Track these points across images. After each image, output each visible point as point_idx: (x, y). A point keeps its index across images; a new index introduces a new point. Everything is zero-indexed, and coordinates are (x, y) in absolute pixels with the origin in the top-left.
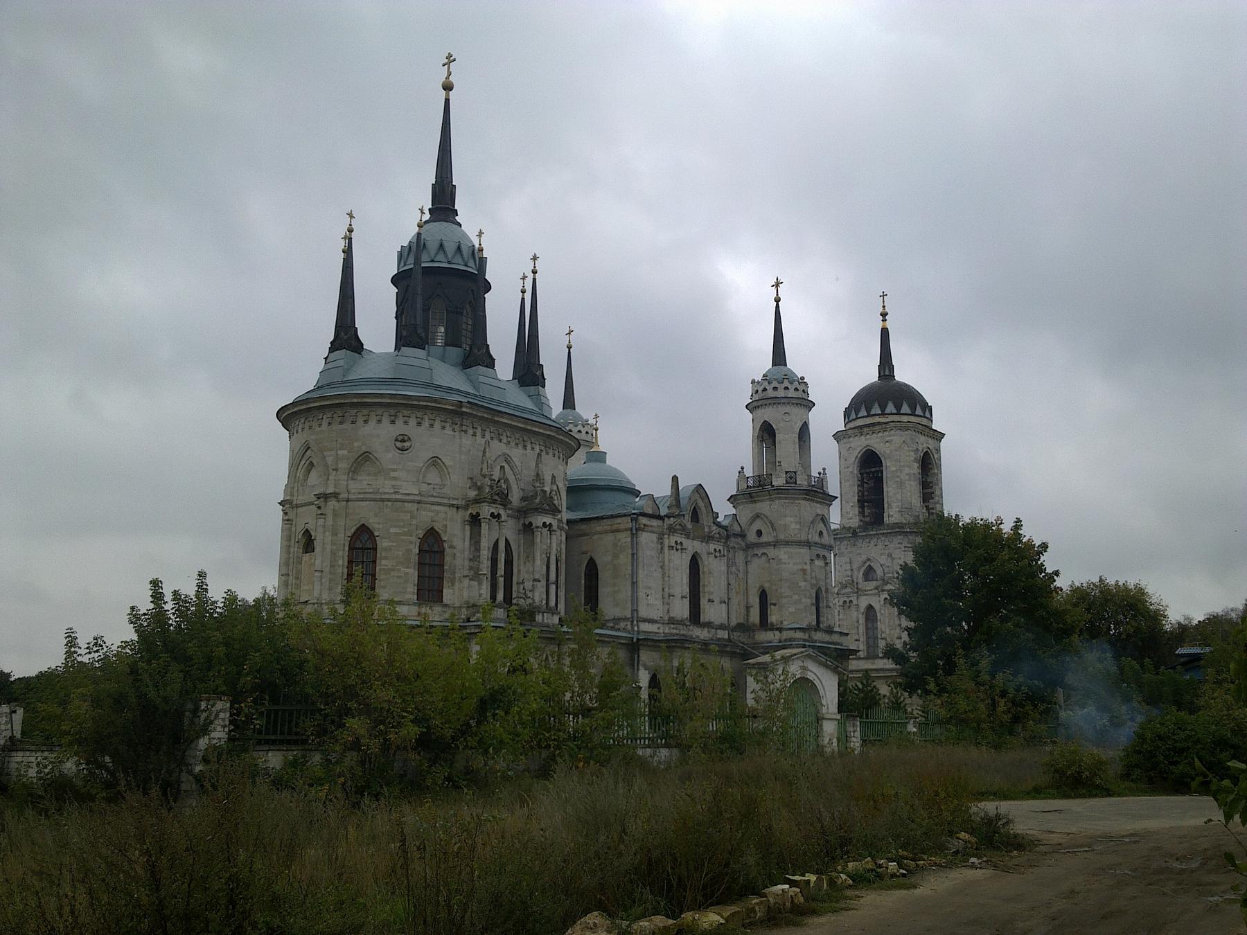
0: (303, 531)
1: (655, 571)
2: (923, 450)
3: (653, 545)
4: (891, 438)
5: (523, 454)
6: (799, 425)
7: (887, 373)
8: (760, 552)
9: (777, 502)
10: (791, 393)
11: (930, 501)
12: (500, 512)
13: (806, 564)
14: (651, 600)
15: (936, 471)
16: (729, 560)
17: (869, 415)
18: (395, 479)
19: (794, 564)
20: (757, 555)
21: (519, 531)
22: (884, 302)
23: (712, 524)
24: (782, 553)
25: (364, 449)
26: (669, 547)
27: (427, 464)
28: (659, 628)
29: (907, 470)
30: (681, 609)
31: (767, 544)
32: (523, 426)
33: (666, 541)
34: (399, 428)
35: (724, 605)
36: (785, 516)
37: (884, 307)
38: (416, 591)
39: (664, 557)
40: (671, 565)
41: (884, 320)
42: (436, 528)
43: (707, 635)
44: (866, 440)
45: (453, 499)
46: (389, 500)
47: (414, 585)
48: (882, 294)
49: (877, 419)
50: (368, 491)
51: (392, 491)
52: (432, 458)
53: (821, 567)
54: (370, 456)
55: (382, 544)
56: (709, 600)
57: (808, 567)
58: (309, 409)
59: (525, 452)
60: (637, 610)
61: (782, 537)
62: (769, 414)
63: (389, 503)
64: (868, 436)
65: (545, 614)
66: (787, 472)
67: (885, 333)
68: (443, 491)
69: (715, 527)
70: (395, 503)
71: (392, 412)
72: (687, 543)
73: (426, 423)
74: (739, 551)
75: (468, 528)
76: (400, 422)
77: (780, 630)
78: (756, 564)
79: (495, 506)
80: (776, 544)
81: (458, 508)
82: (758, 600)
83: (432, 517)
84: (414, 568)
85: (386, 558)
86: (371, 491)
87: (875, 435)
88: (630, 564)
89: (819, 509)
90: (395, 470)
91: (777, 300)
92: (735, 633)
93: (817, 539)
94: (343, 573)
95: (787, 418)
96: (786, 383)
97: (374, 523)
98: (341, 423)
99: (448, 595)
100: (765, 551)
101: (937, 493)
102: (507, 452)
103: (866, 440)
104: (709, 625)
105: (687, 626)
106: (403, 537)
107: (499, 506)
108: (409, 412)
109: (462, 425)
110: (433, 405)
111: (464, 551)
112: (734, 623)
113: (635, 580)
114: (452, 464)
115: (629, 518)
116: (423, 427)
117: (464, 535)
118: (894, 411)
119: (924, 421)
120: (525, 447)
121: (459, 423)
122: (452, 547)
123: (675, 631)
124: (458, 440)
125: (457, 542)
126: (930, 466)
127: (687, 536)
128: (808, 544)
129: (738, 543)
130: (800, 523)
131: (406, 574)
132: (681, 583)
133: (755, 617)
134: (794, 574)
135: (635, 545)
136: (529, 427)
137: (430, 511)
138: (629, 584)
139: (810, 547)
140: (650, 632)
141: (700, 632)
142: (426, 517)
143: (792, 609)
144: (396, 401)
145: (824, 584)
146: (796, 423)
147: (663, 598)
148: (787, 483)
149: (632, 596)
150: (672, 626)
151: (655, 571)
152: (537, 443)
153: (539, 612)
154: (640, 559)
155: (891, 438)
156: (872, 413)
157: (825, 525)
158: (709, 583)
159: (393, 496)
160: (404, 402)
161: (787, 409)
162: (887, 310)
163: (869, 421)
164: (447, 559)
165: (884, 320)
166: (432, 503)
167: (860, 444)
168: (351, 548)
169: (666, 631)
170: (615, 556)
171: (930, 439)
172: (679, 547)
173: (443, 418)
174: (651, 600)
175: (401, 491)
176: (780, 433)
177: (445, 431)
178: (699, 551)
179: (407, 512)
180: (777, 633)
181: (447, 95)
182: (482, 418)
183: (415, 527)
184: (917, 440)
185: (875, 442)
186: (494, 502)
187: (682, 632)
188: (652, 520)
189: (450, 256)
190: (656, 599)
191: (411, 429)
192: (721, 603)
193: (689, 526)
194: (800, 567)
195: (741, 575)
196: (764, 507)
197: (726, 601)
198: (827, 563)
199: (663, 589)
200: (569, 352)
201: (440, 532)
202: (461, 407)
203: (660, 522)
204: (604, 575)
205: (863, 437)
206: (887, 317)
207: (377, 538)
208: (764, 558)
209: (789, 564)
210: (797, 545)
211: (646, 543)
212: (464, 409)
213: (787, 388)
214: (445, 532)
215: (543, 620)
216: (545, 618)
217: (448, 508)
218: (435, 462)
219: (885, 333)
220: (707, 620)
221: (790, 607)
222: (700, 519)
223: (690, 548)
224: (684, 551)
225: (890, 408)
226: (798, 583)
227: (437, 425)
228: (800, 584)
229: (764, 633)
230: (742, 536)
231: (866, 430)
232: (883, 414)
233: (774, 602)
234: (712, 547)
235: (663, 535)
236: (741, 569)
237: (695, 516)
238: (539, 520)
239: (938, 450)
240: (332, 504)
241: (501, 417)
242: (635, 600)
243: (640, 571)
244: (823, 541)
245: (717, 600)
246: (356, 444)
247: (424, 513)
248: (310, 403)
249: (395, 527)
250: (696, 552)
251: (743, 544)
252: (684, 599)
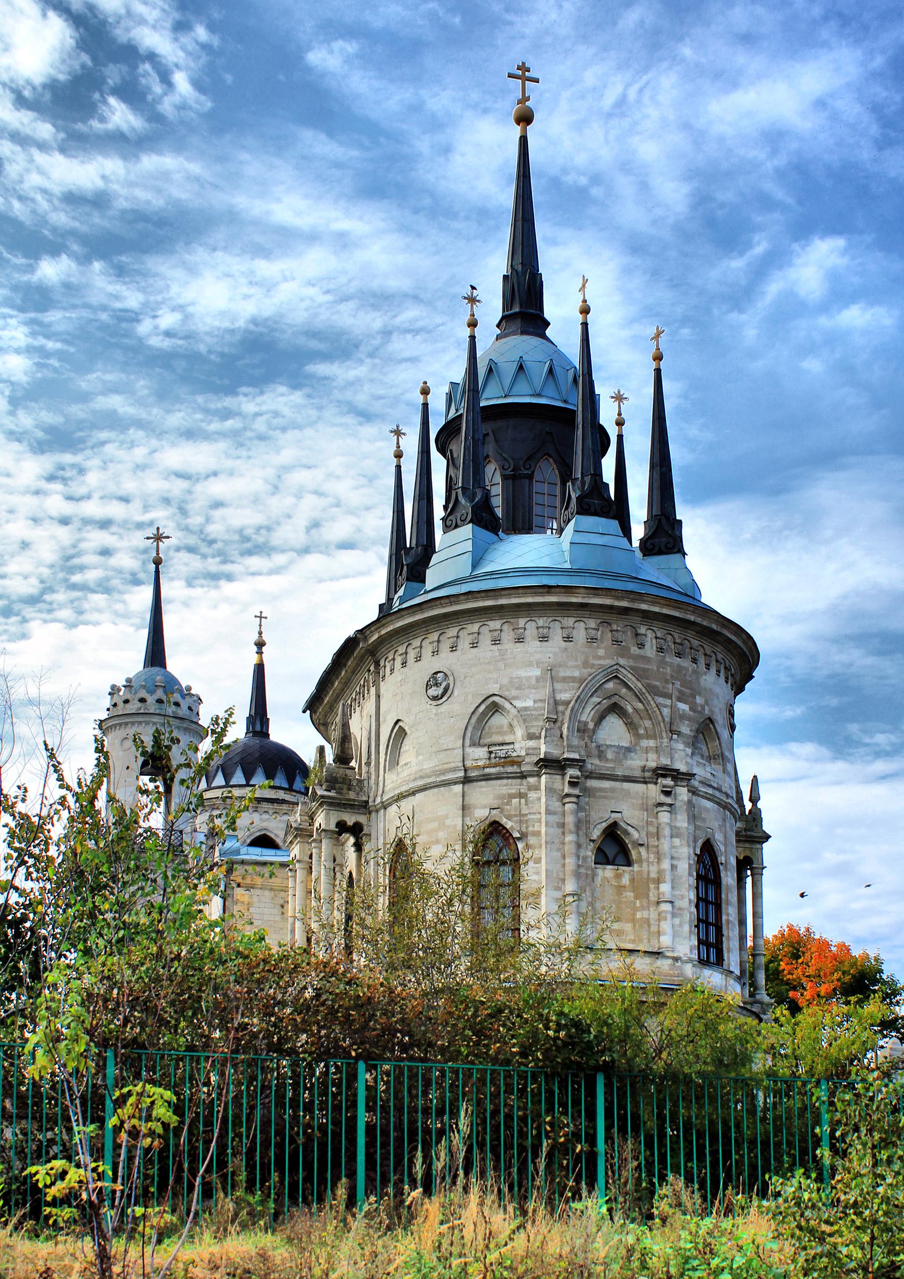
0: (604, 825)
22: (260, 625)
37: (260, 633)
41: (260, 653)
48: (259, 615)
54: (711, 726)
58: (626, 611)
67: (259, 671)
165: (260, 653)
206: (264, 649)
219: (259, 671)
240: (682, 793)
248: (644, 602)
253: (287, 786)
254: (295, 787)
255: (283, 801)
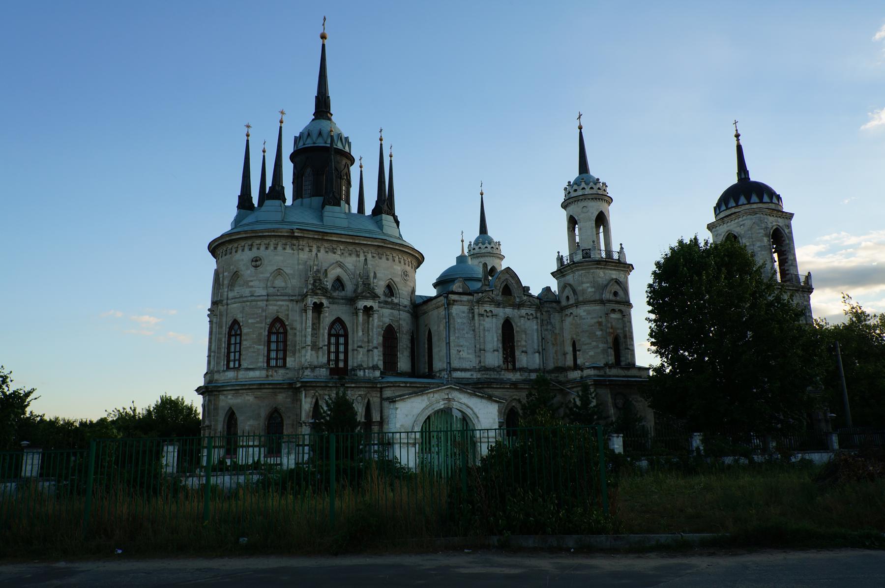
1: (467, 333)
2: (772, 227)
3: (464, 315)
4: (744, 222)
5: (356, 260)
6: (596, 214)
7: (743, 176)
8: (568, 312)
9: (576, 273)
10: (588, 191)
11: (786, 264)
12: (323, 301)
13: (601, 317)
14: (464, 354)
15: (788, 242)
16: (542, 320)
17: (727, 208)
18: (252, 287)
19: (592, 318)
20: (567, 315)
21: (353, 313)
22: (736, 127)
23: (523, 296)
24: (581, 311)
25: (235, 270)
26: (479, 315)
27: (273, 275)
28: (472, 375)
29: (758, 244)
30: (494, 359)
31: (572, 306)
32: (351, 241)
33: (476, 311)
34: (254, 253)
35: (537, 355)
36: (582, 283)
37: (737, 130)
38: (265, 360)
39: (474, 324)
40: (482, 328)
41: (738, 140)
42: (280, 317)
43: (520, 377)
44: (728, 226)
45: (292, 296)
46: (248, 301)
47: (264, 356)
49: (733, 210)
50: (237, 297)
51: (249, 295)
52: (277, 270)
53: (618, 319)
55: (245, 330)
56: (523, 352)
57: (603, 320)
59: (358, 259)
60: (450, 363)
61: (581, 299)
62: (575, 209)
63: (248, 303)
64: (729, 224)
65: (366, 371)
66: (583, 250)
67: (739, 149)
68: (285, 291)
69: (525, 298)
70: (252, 303)
71: (250, 242)
72: (496, 310)
73: (272, 247)
74: (553, 313)
75: (304, 314)
76: (254, 249)
77: (582, 370)
78: (569, 320)
79: (318, 297)
80: (577, 304)
81: (297, 302)
82: (571, 349)
83: (277, 310)
84: (264, 345)
85: (246, 340)
86: (239, 296)
87: (733, 222)
88: (445, 329)
89: (614, 274)
90: (252, 281)
91: (580, 128)
92: (553, 375)
93: (612, 297)
94: (224, 352)
95: (584, 210)
96: (583, 185)
97: (239, 318)
98: (225, 255)
99: (290, 362)
100: (571, 311)
101: (790, 257)
102: (341, 260)
103: (728, 226)
104: (522, 370)
105: (497, 372)
106: (256, 325)
107: (320, 297)
108: (260, 241)
109: (299, 245)
110: (273, 234)
111: (302, 331)
112: (551, 365)
113: (448, 342)
114: (292, 272)
115: (442, 297)
116: (269, 250)
117: (302, 319)
118: (746, 202)
119: (773, 206)
120: (358, 256)
121: (297, 244)
122: (292, 329)
123: (485, 376)
124: (297, 256)
125: (298, 327)
126: (783, 239)
127: (498, 305)
128: (602, 302)
129: (552, 308)
130: (594, 287)
131: (258, 349)
132: (493, 339)
133: (570, 362)
134: (591, 326)
135: (449, 316)
136: (357, 241)
137: (275, 305)
138: (445, 343)
139: (604, 304)
140: (463, 378)
141: (512, 375)
142: (273, 309)
143: (591, 353)
144: (248, 235)
145: (622, 331)
146: (592, 213)
147: (475, 352)
148: (583, 258)
149: (447, 353)
150: (483, 372)
151: (467, 333)
152: (370, 252)
153: (360, 370)
154: (451, 326)
155: (744, 222)
156: (729, 207)
157: (620, 286)
158: (522, 339)
159: (250, 298)
160: (254, 235)
161: (585, 203)
162: (739, 132)
163: (728, 212)
164: (290, 337)
165: (738, 140)
166: (277, 301)
167: (723, 229)
168: (230, 336)
169: (479, 377)
170: (439, 327)
171: (779, 219)
172: (490, 314)
173: (284, 242)
174: (464, 354)
175: (255, 294)
176: (580, 222)
177: (286, 251)
178: (510, 316)
179: (260, 308)
180: (579, 372)
181: (323, 41)
182: (314, 239)
183: (264, 318)
184: (766, 221)
185: (733, 226)
186: (316, 294)
187: (492, 377)
188: (462, 296)
189: (314, 139)
190: (468, 354)
191: (262, 253)
192: (535, 353)
193: (500, 298)
194: (595, 320)
195: (557, 331)
196: (570, 278)
197: (541, 350)
198: (624, 316)
199: (475, 346)
200: (482, 198)
201: (284, 319)
202: (294, 233)
203: (470, 297)
204: (435, 339)
205: (725, 225)
206: (740, 138)
207: (242, 327)
208: (572, 316)
209: (587, 318)
210: (593, 304)
211: (456, 314)
212: (296, 234)
213: (584, 188)
214: (288, 319)
215: (364, 374)
216: (367, 374)
217: (289, 302)
218: (279, 272)
219: (739, 149)
220: (521, 366)
221: (590, 352)
222: (512, 293)
223: (501, 314)
224: (494, 316)
225: (743, 200)
226: (595, 333)
227: (280, 248)
228: (597, 334)
229: (572, 373)
230: (558, 302)
231: (725, 219)
232: (737, 206)
233: (578, 349)
234: (523, 312)
235: (474, 306)
236: (558, 326)
237: (507, 291)
238: (361, 304)
239: (789, 226)
241: (331, 237)
242: (449, 355)
243: (451, 334)
244: (618, 298)
245: (529, 352)
246: (231, 268)
247: (271, 307)
249: (252, 319)
250: (508, 317)
251: (558, 308)
252: (496, 353)
253: (735, 205)
254: (752, 202)
255: (735, 213)
